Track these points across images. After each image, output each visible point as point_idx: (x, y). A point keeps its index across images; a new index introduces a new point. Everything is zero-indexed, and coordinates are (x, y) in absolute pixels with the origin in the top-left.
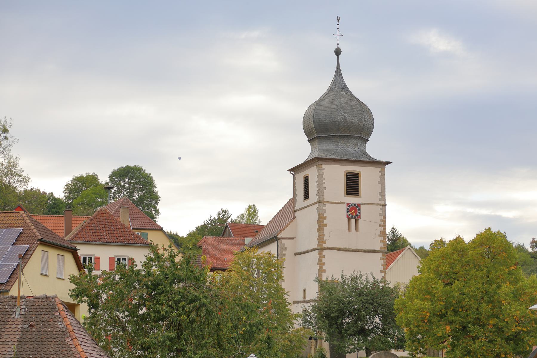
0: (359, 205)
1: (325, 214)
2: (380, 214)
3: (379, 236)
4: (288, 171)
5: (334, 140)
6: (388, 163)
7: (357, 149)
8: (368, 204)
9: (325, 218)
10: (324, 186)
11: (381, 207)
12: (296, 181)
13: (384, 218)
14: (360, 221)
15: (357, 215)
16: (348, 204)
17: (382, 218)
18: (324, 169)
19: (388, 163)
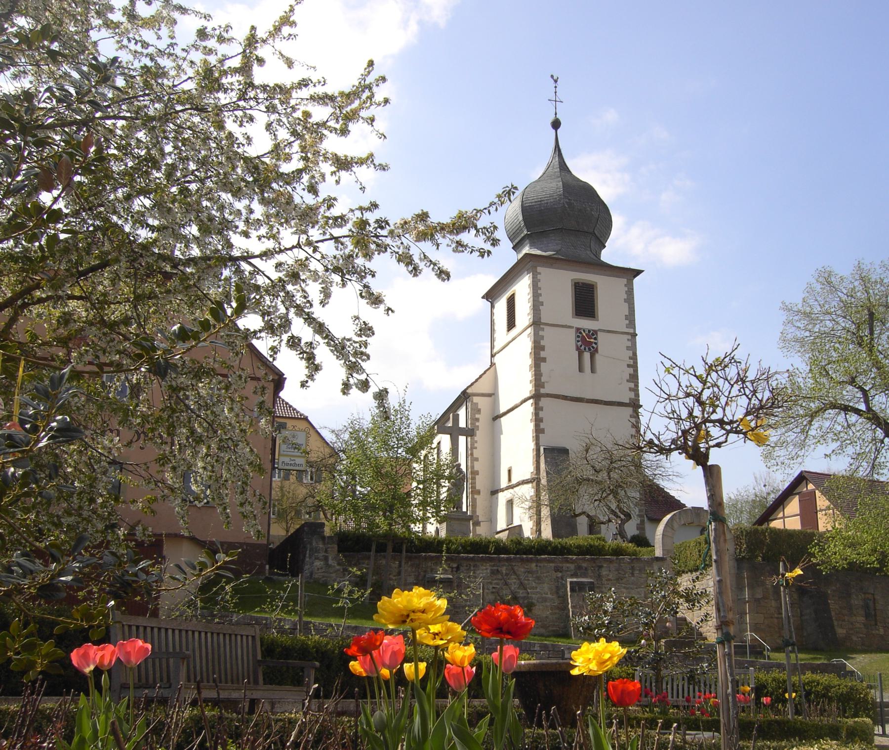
0: (595, 332)
2: (628, 348)
3: (628, 381)
4: (483, 297)
5: (553, 238)
6: (638, 272)
7: (589, 252)
8: (609, 332)
9: (543, 348)
10: (541, 299)
12: (495, 311)
13: (635, 354)
14: (597, 356)
15: (593, 347)
16: (578, 330)
17: (630, 353)
18: (540, 273)
19: (638, 272)
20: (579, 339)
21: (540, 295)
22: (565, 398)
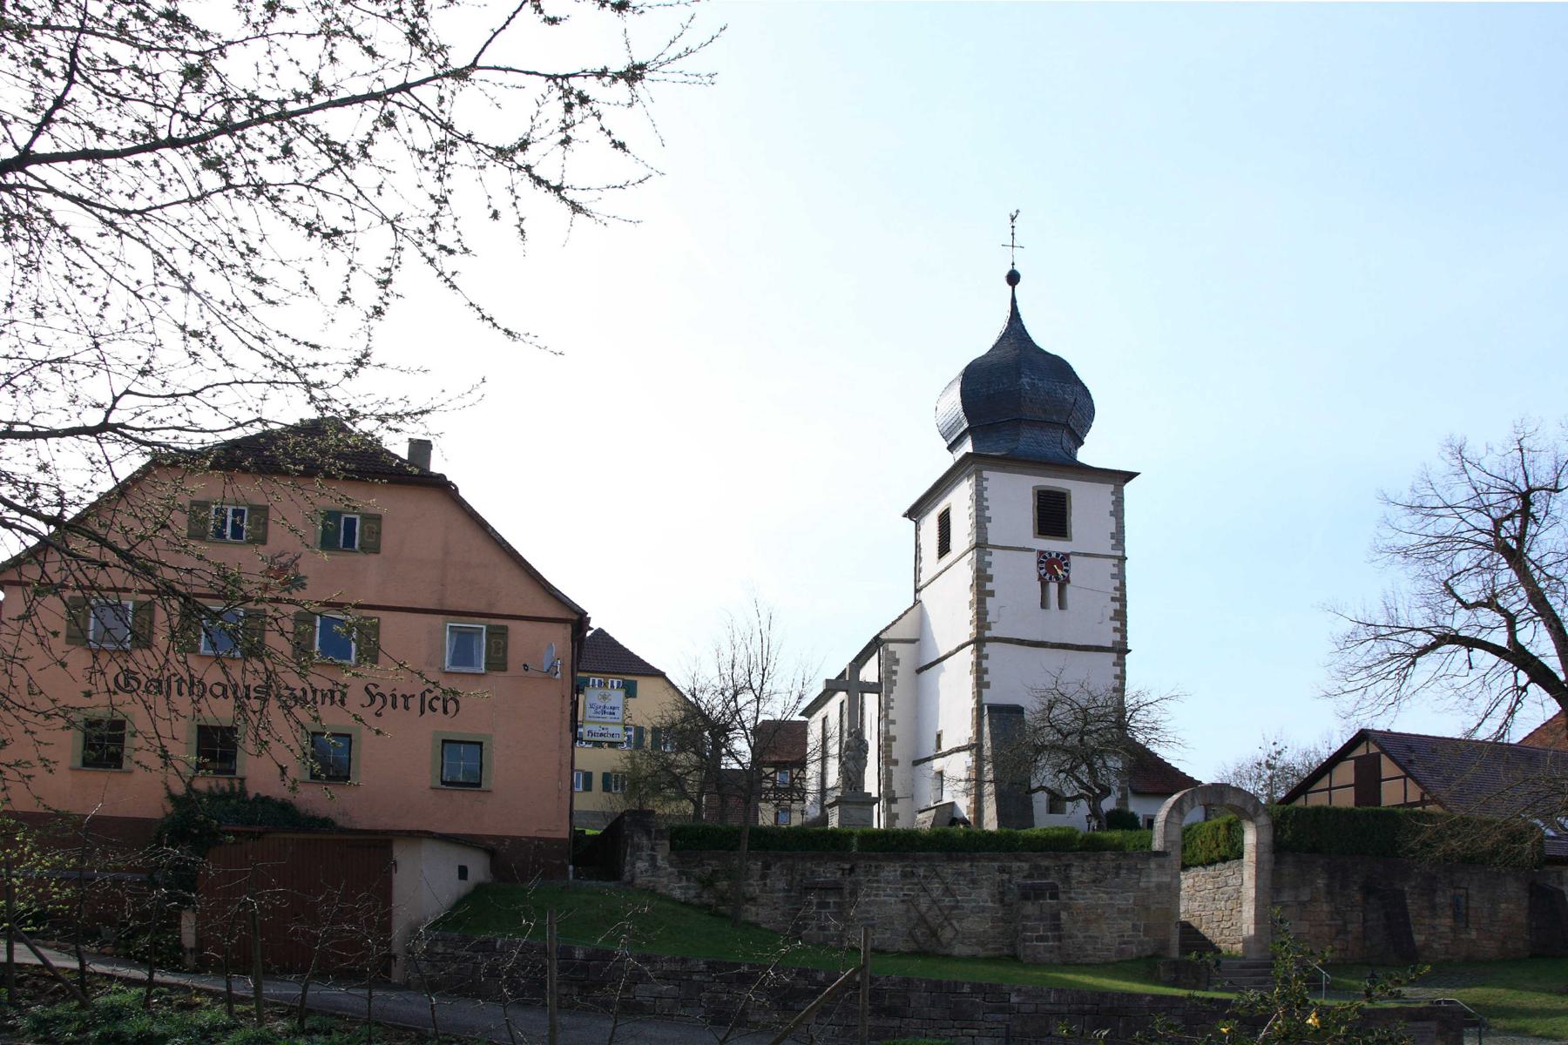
0: (1066, 556)
1: (989, 571)
2: (1113, 576)
6: (1130, 476)
8: (1086, 555)
9: (990, 578)
10: (988, 514)
11: (1116, 561)
13: (1123, 584)
14: (1070, 589)
16: (1041, 553)
17: (1117, 583)
18: (987, 479)
19: (1130, 476)
20: (1043, 565)
21: (988, 508)
22: (1021, 642)
